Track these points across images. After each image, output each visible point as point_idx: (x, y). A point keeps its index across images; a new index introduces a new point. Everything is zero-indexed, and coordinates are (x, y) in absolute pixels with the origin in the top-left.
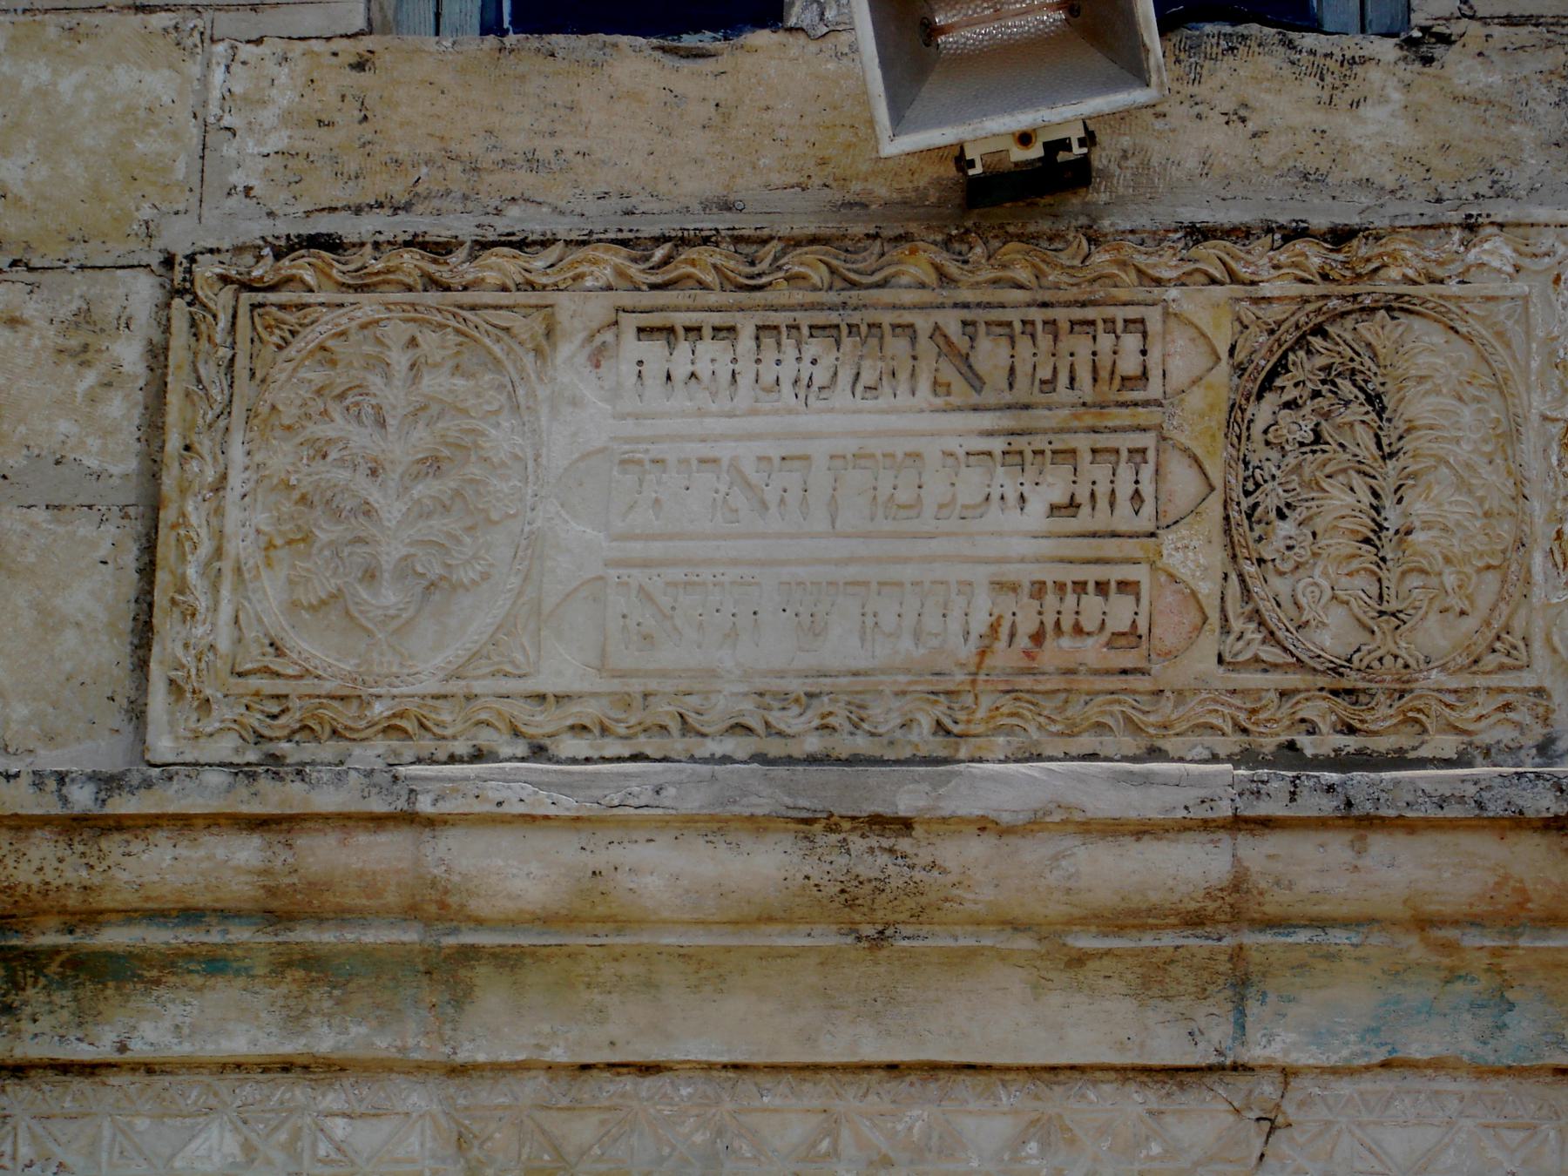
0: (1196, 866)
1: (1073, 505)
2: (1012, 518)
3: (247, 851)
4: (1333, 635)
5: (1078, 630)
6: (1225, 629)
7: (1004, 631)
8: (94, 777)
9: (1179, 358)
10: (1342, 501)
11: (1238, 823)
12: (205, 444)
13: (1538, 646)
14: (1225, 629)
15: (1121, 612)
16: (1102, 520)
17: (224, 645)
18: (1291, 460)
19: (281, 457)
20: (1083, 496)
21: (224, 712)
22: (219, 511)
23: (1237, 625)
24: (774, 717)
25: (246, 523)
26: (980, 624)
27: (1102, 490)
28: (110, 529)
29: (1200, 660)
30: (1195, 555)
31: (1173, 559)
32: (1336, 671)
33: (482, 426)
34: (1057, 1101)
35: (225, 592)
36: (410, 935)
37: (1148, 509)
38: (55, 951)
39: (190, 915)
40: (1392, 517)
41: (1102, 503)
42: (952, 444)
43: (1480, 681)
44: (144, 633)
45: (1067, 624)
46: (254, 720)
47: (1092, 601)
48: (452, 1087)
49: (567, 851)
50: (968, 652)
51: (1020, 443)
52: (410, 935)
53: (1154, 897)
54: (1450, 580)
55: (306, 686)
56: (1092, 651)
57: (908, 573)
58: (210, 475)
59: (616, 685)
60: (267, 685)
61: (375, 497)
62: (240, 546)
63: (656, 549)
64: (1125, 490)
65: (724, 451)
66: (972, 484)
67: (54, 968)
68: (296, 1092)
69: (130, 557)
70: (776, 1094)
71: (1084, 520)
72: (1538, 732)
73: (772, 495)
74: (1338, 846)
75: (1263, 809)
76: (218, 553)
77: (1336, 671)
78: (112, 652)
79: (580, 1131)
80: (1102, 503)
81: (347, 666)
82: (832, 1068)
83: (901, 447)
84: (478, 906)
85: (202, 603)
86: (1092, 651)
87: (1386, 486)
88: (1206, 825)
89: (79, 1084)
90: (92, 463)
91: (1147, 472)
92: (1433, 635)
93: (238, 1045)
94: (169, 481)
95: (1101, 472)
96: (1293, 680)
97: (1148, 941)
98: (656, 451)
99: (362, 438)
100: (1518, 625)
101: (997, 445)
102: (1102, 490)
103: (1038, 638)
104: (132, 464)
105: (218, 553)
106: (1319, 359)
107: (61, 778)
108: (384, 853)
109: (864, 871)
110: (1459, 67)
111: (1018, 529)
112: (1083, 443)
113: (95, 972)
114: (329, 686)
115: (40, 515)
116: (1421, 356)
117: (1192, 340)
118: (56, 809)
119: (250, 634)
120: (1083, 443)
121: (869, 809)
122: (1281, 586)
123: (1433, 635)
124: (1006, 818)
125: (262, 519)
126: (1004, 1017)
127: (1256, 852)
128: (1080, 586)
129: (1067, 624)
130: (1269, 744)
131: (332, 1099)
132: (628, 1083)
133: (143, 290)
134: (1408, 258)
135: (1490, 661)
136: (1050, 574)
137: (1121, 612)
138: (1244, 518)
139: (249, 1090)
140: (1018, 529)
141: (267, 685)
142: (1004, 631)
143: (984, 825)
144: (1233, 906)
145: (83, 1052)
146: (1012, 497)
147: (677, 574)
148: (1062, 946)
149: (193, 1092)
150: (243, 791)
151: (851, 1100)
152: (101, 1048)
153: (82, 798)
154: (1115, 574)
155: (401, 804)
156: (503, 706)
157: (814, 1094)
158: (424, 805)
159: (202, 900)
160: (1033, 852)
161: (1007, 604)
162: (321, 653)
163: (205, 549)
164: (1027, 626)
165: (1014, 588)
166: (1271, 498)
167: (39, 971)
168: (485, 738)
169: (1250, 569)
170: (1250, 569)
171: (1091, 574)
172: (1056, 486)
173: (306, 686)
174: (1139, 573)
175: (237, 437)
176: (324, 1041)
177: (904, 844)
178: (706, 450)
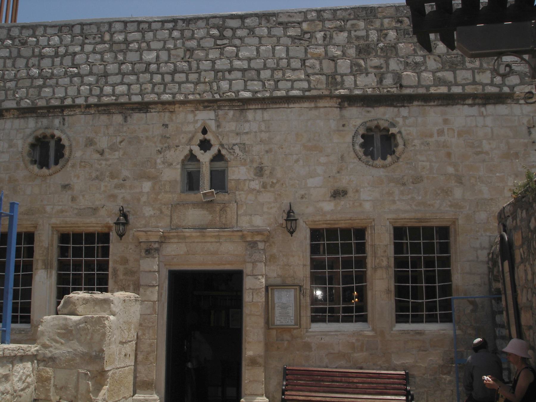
0: (217, 234)
4: (224, 222)
9: (217, 209)
10: (224, 216)
30: (218, 219)
106: (223, 210)
108: (182, 233)
110: (230, 195)
113: (170, 238)
116: (228, 209)
117: (218, 208)
123: (228, 222)
126: (209, 240)
133: (170, 206)
134: (227, 205)
138: (220, 217)
140: (210, 217)
144: (218, 235)
148: (211, 237)
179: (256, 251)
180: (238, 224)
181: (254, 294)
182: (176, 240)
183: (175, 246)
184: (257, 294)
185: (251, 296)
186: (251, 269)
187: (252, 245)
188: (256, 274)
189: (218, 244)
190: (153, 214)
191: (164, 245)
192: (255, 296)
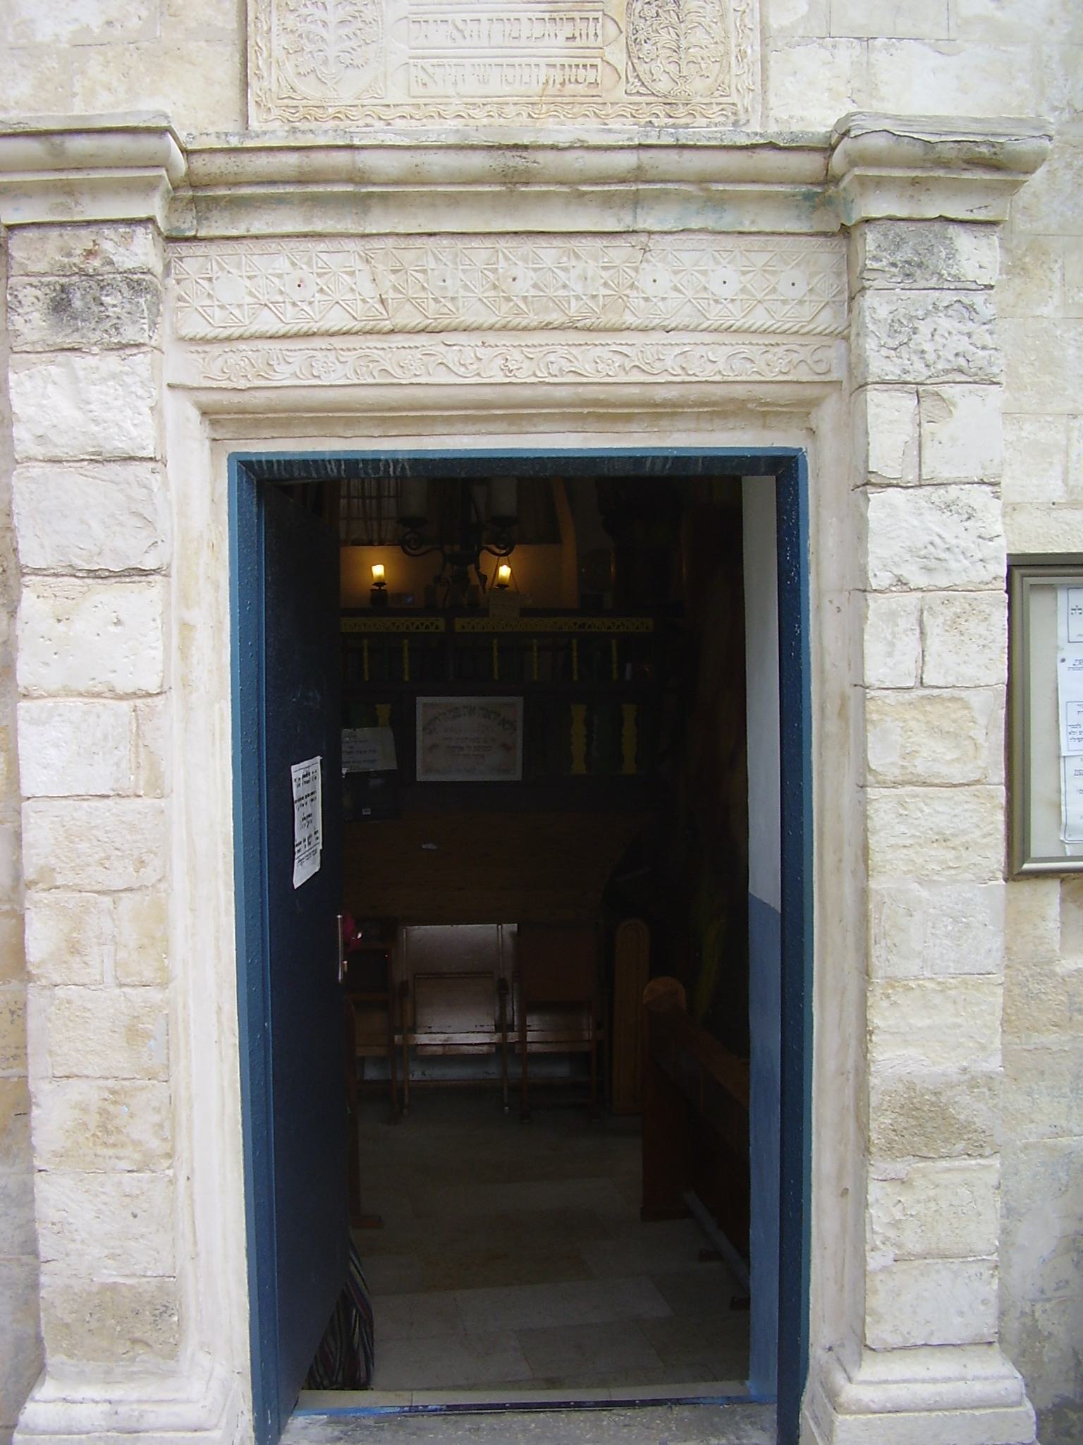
0: (626, 160)
1: (574, 38)
2: (553, 42)
3: (293, 159)
4: (664, 85)
5: (577, 81)
6: (628, 82)
7: (551, 82)
8: (238, 134)
10: (666, 37)
11: (641, 147)
12: (262, 17)
13: (733, 87)
14: (628, 82)
15: (591, 75)
16: (583, 43)
17: (274, 89)
18: (648, 23)
19: (291, 21)
20: (577, 35)
21: (276, 112)
22: (270, 41)
23: (631, 80)
24: (471, 112)
25: (280, 42)
26: (543, 80)
27: (584, 32)
28: (229, 48)
29: (619, 94)
30: (617, 56)
31: (608, 57)
32: (665, 96)
33: (363, 9)
34: (575, 243)
35: (273, 70)
36: (350, 188)
37: (600, 38)
38: (224, 196)
39: (273, 183)
40: (684, 43)
41: (584, 37)
42: (530, 15)
43: (713, 100)
44: (245, 84)
45: (573, 80)
46: (287, 115)
47: (581, 70)
48: (363, 242)
49: (406, 158)
50: (537, 89)
51: (554, 15)
52: (350, 188)
53: (610, 172)
54: (703, 66)
55: (304, 102)
56: (581, 89)
57: (516, 61)
58: (265, 28)
59: (414, 101)
60: (291, 103)
61: (325, 35)
62: (278, 53)
63: (426, 52)
64: (591, 33)
65: (448, 17)
66: (538, 29)
67: (223, 204)
68: (309, 245)
69: (237, 58)
70: (476, 243)
71: (578, 43)
72: (732, 118)
73: (467, 34)
74: (673, 155)
75: (649, 142)
76: (270, 56)
77: (665, 96)
78: (233, 93)
79: (409, 256)
80: (584, 37)
81: (318, 95)
82: (495, 233)
83: (512, 16)
84: (374, 178)
85: (265, 75)
86: (581, 89)
87: (681, 33)
88: (630, 147)
89: (231, 243)
90: (220, 25)
91: (599, 25)
92: (698, 85)
93: (289, 228)
94: (251, 29)
95: (583, 25)
96: (652, 99)
97: (606, 188)
98: (426, 17)
99: (319, 13)
100: (727, 82)
101: (547, 16)
102: (584, 32)
103: (563, 84)
104: (235, 25)
105: (270, 56)
107: (226, 134)
108: (342, 158)
109: (511, 164)
111: (555, 45)
112: (576, 15)
114: (311, 103)
115: (202, 44)
118: (226, 146)
119: (283, 84)
120: (576, 15)
121: (512, 142)
122: (647, 67)
123: (698, 85)
124: (561, 145)
125: (283, 42)
127: (646, 156)
128: (577, 66)
129: (573, 80)
130: (643, 122)
131: (322, 246)
132: (425, 239)
135: (717, 94)
136: (566, 61)
137: (591, 75)
138: (634, 43)
139: (293, 244)
141: (291, 103)
142: (551, 82)
143: (554, 147)
145: (235, 233)
146: (552, 35)
147: (435, 61)
149: (274, 246)
150: (291, 138)
151: (502, 243)
152: (242, 232)
153: (234, 142)
154: (589, 62)
155: (348, 142)
156: (376, 109)
157: (488, 242)
158: (356, 142)
159: (276, 178)
160: (569, 156)
161: (552, 70)
162: (309, 89)
163: (265, 54)
164: (559, 80)
165: (554, 66)
166: (641, 37)
167: (218, 204)
168: (369, 120)
169: (635, 61)
170: (635, 61)
171: (581, 61)
172: (568, 30)
173: (304, 102)
174: (598, 61)
175: (274, 13)
176: (319, 227)
177: (524, 154)
178: (443, 17)
179: (949, 297)
180: (773, 101)
181: (934, 626)
182: (291, 222)
183: (282, 264)
184: (954, 624)
185: (910, 644)
186: (906, 432)
187: (906, 253)
188: (945, 474)
189: (620, 252)
190: (96, 24)
191: (193, 261)
192: (933, 644)
